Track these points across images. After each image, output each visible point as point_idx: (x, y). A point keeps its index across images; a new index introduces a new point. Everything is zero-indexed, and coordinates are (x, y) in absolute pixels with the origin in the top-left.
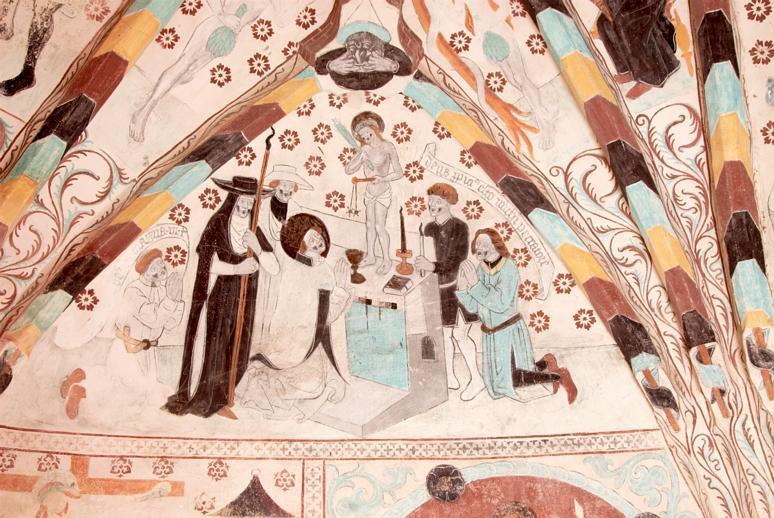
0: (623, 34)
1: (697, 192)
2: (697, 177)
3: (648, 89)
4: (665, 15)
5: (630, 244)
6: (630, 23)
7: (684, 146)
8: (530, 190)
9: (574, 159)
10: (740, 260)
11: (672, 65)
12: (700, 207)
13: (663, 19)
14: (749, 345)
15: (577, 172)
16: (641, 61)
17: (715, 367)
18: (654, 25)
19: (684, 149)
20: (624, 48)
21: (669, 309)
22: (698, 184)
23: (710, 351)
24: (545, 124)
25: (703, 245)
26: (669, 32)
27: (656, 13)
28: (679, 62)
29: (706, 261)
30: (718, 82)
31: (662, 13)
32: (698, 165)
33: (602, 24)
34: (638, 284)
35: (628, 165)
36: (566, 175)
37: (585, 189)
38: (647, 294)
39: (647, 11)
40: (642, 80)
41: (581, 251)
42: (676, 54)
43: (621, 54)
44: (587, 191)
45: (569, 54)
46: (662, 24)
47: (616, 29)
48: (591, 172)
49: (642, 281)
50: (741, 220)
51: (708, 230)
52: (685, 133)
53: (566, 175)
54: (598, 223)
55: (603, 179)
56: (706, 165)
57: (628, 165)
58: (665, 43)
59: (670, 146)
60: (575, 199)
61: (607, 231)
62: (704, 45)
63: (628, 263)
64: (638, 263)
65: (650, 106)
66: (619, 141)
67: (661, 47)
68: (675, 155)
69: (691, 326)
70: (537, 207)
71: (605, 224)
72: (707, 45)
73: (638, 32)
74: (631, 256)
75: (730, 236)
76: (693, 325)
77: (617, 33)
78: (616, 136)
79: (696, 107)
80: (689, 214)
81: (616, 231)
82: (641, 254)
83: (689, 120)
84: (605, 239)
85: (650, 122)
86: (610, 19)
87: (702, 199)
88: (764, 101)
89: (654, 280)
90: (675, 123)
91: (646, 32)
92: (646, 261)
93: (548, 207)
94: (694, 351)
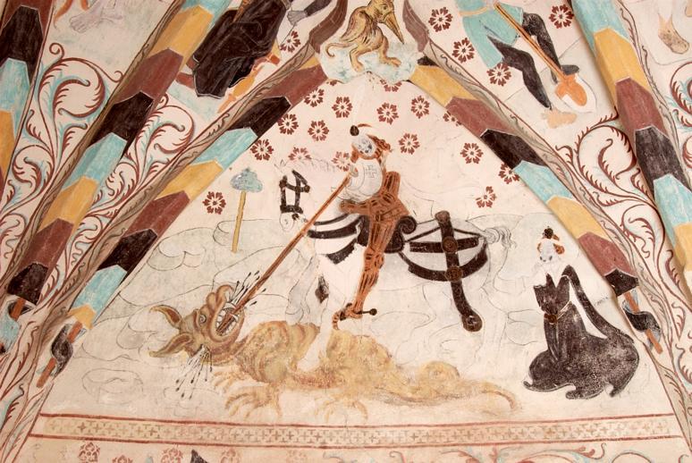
0: (226, 37)
1: (128, 182)
2: (140, 174)
3: (191, 87)
4: (256, 61)
5: (39, 163)
6: (238, 38)
7: (160, 146)
8: (36, 44)
9: (82, 61)
10: (120, 265)
11: (218, 92)
12: (118, 194)
13: (252, 62)
14: (63, 331)
15: (71, 70)
16: (210, 66)
17: (16, 325)
18: (244, 57)
19: (158, 149)
20: (215, 45)
21: (14, 244)
22: (135, 179)
23: (25, 309)
24: (98, 12)
25: (90, 222)
26: (244, 72)
27: (254, 53)
28: (224, 95)
29: (79, 235)
30: (238, 141)
31: (256, 58)
32: (151, 168)
33: (229, 16)
34: (9, 200)
35: (126, 115)
36: (60, 62)
37: (60, 87)
38: (8, 215)
39: (252, 45)
40: (197, 77)
41: (11, 129)
42: (228, 89)
43: (211, 46)
44: (59, 91)
45: (207, 10)
46: (247, 64)
47: (229, 29)
48: (80, 83)
49: (16, 200)
50: (149, 238)
51: (104, 216)
52: (171, 139)
53: (60, 62)
54: (35, 122)
55: (81, 100)
56: (155, 173)
57: (126, 115)
58: (233, 75)
59: (153, 136)
60: (41, 85)
61: (35, 136)
62: (258, 110)
63: (20, 176)
64: (27, 185)
65: (177, 97)
66: (151, 100)
67: (228, 73)
68: (149, 145)
69: (31, 277)
70: (27, 62)
71: (40, 129)
72: (260, 113)
73: (233, 48)
74: (29, 173)
75: (131, 241)
76: (34, 278)
77: (226, 33)
78: (155, 95)
79: (196, 134)
80: (106, 191)
81: (41, 145)
82: (38, 181)
83: (183, 135)
84: (25, 140)
85: (165, 106)
86: (235, 20)
87: (125, 191)
88: (231, 176)
89: (28, 210)
90: (175, 126)
91: (235, 55)
92: (36, 189)
93: (31, 71)
94: (13, 298)
